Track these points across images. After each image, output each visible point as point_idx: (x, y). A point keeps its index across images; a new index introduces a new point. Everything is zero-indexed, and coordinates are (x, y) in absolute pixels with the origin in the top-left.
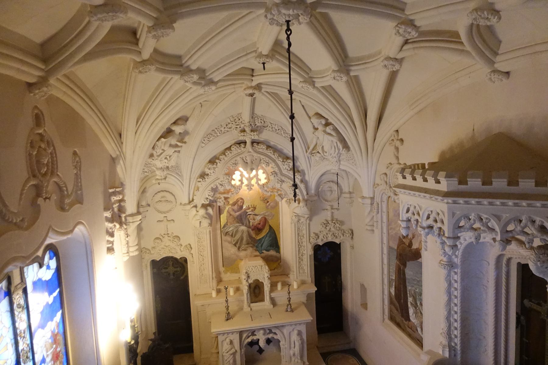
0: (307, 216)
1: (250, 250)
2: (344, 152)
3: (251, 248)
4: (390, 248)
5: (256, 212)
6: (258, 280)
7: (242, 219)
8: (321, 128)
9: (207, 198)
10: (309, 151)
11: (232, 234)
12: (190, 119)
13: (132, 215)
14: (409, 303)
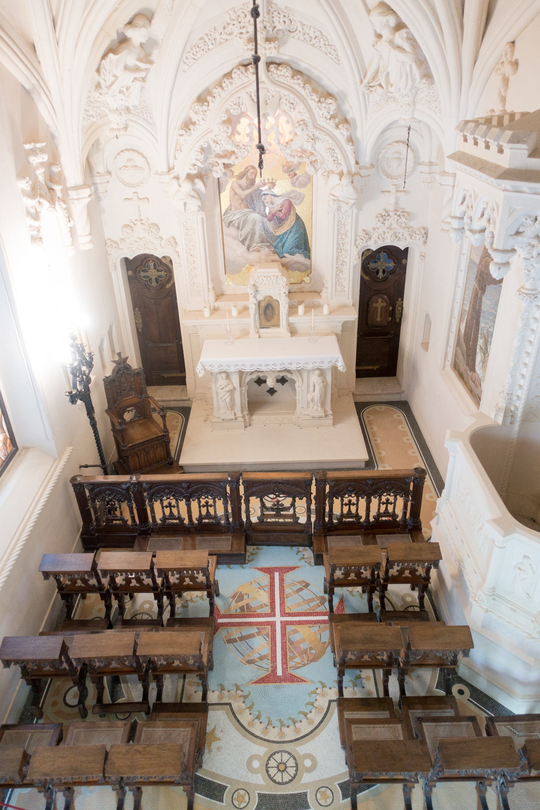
0: (352, 202)
1: (266, 251)
2: (422, 84)
3: (267, 250)
4: (471, 262)
5: (276, 191)
6: (272, 298)
8: (386, 34)
9: (195, 165)
10: (365, 82)
11: (239, 224)
12: (156, 16)
13: (76, 188)
14: (478, 347)
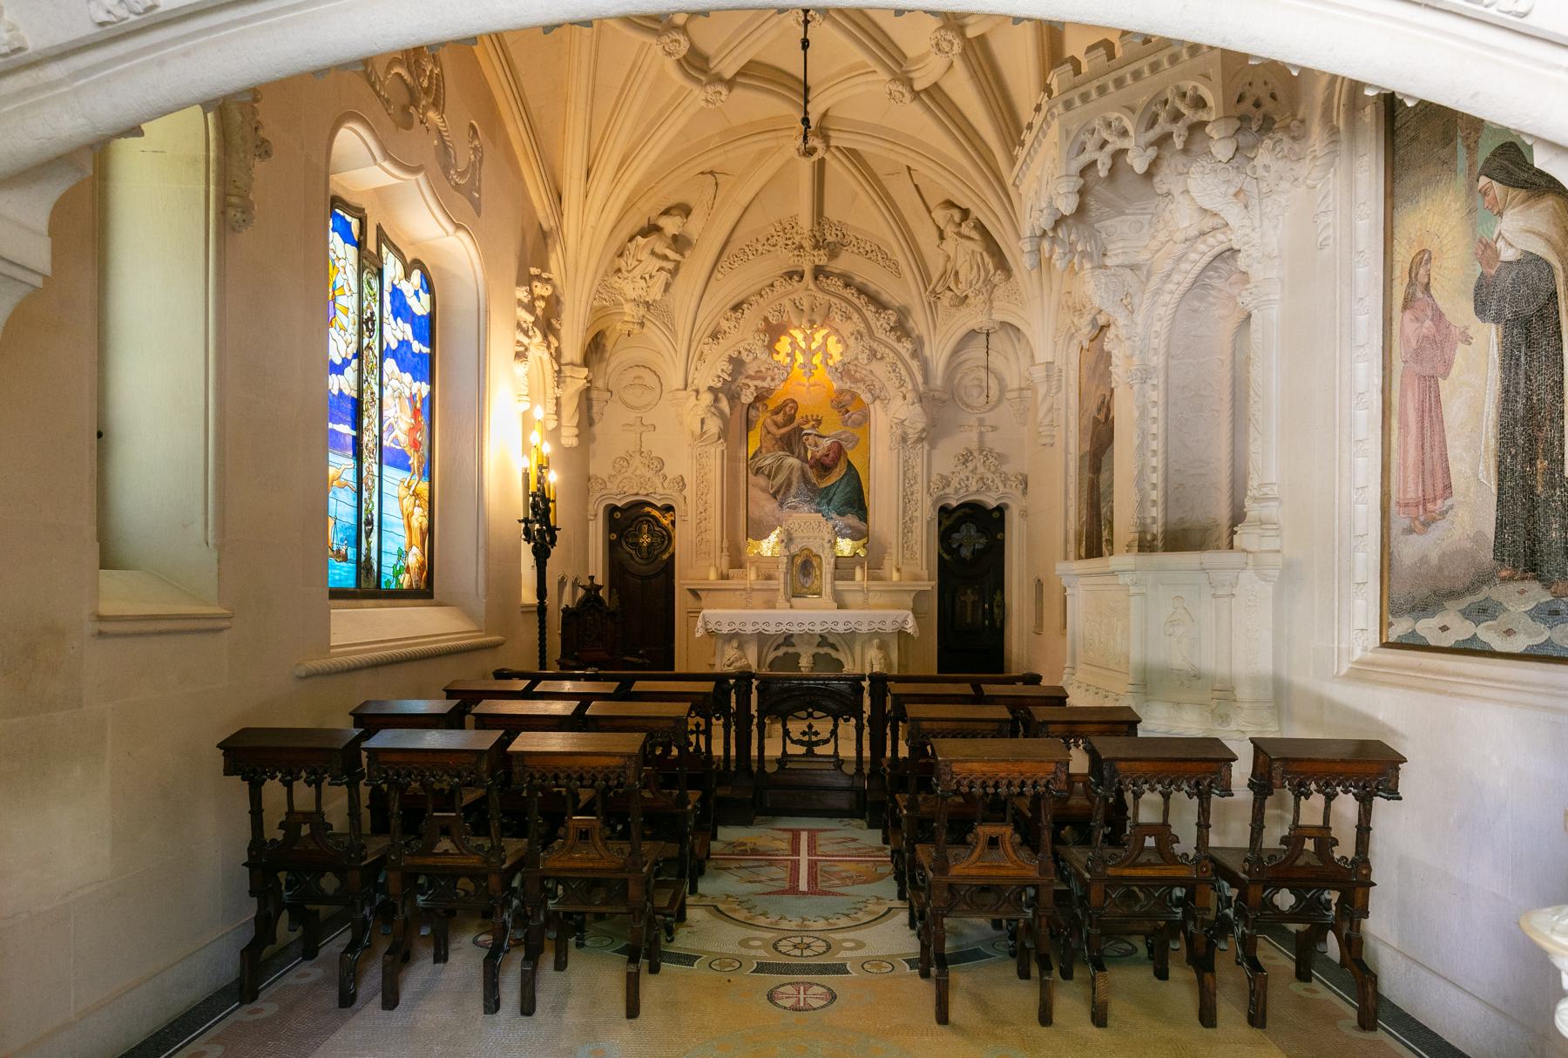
0: (920, 426)
2: (998, 277)
4: (1081, 457)
5: (822, 430)
7: (791, 441)
8: (949, 230)
